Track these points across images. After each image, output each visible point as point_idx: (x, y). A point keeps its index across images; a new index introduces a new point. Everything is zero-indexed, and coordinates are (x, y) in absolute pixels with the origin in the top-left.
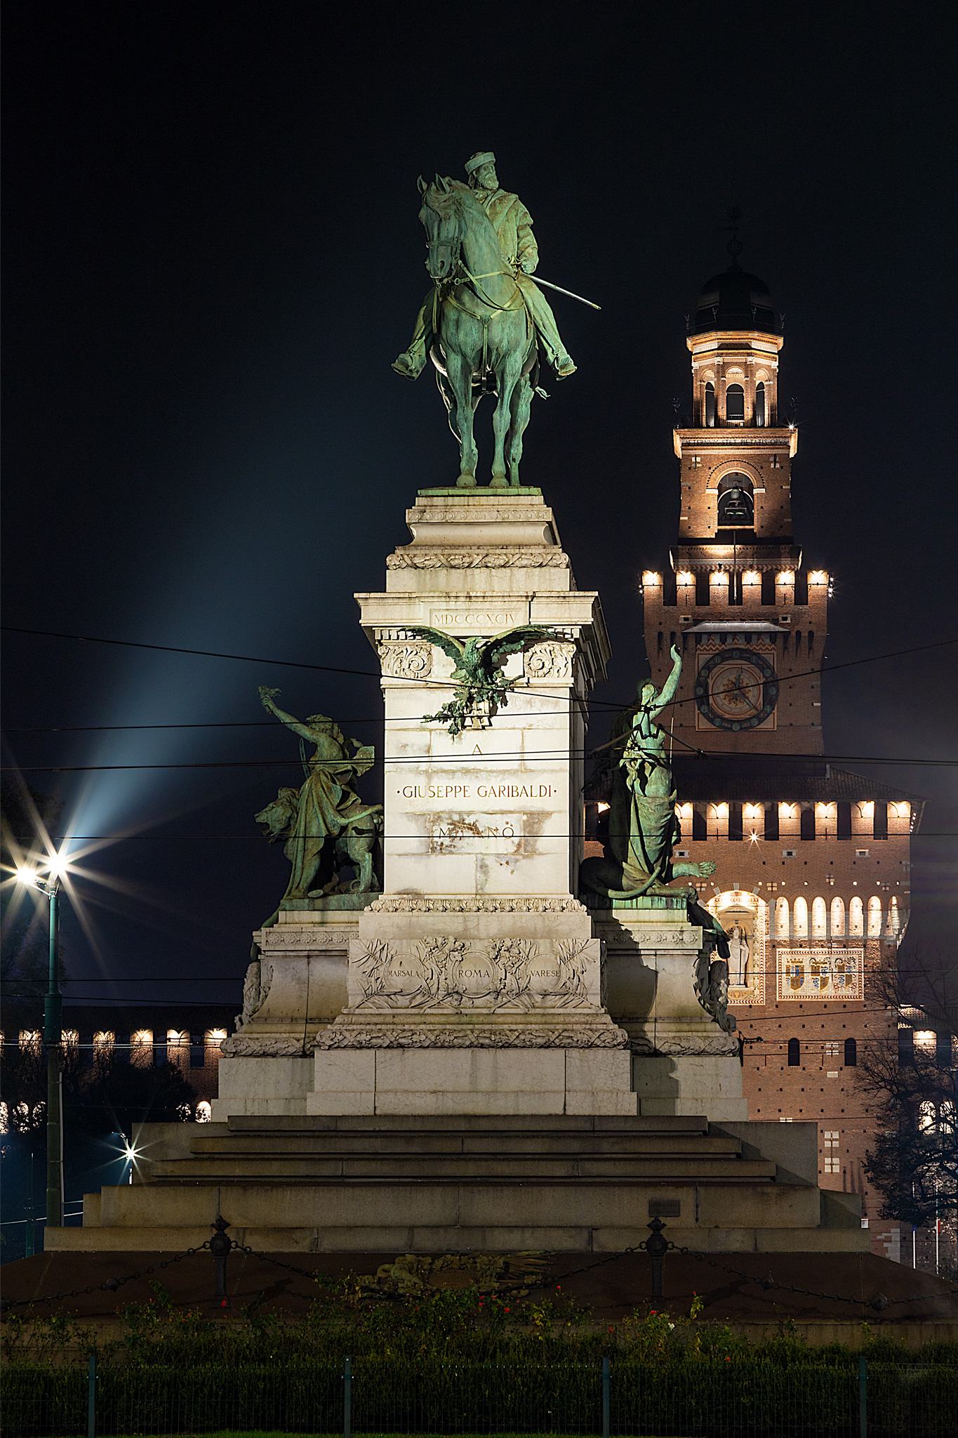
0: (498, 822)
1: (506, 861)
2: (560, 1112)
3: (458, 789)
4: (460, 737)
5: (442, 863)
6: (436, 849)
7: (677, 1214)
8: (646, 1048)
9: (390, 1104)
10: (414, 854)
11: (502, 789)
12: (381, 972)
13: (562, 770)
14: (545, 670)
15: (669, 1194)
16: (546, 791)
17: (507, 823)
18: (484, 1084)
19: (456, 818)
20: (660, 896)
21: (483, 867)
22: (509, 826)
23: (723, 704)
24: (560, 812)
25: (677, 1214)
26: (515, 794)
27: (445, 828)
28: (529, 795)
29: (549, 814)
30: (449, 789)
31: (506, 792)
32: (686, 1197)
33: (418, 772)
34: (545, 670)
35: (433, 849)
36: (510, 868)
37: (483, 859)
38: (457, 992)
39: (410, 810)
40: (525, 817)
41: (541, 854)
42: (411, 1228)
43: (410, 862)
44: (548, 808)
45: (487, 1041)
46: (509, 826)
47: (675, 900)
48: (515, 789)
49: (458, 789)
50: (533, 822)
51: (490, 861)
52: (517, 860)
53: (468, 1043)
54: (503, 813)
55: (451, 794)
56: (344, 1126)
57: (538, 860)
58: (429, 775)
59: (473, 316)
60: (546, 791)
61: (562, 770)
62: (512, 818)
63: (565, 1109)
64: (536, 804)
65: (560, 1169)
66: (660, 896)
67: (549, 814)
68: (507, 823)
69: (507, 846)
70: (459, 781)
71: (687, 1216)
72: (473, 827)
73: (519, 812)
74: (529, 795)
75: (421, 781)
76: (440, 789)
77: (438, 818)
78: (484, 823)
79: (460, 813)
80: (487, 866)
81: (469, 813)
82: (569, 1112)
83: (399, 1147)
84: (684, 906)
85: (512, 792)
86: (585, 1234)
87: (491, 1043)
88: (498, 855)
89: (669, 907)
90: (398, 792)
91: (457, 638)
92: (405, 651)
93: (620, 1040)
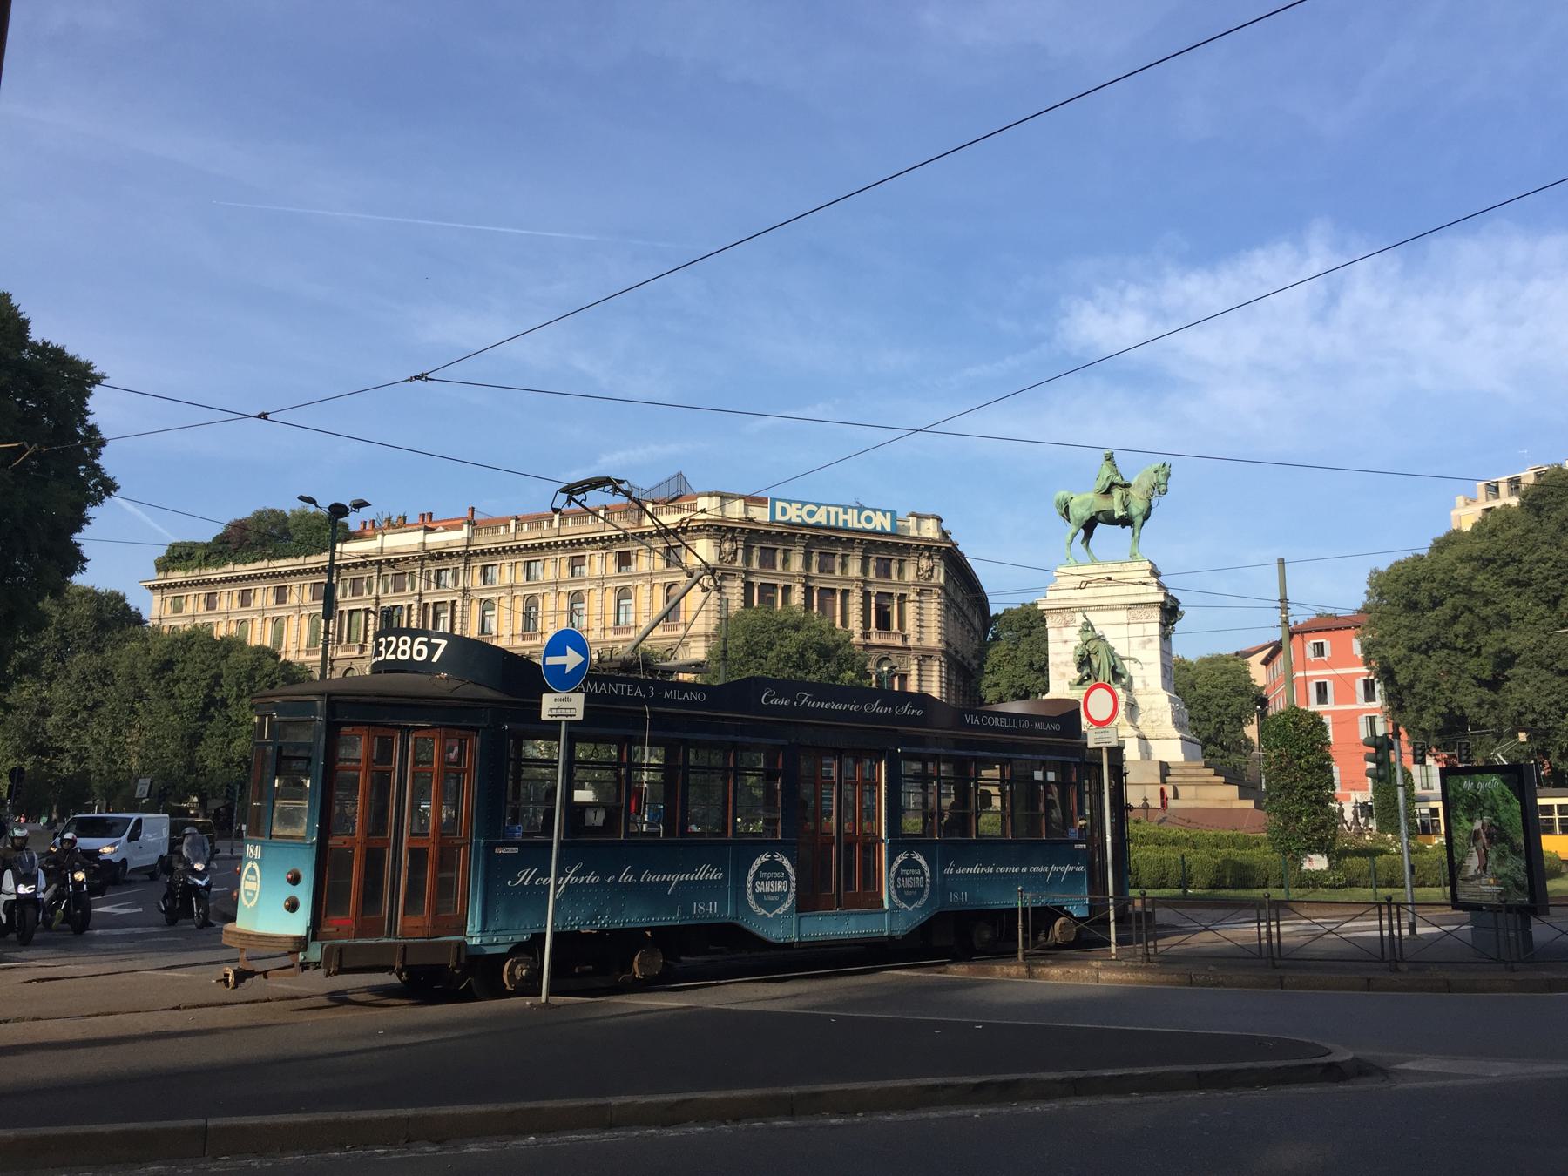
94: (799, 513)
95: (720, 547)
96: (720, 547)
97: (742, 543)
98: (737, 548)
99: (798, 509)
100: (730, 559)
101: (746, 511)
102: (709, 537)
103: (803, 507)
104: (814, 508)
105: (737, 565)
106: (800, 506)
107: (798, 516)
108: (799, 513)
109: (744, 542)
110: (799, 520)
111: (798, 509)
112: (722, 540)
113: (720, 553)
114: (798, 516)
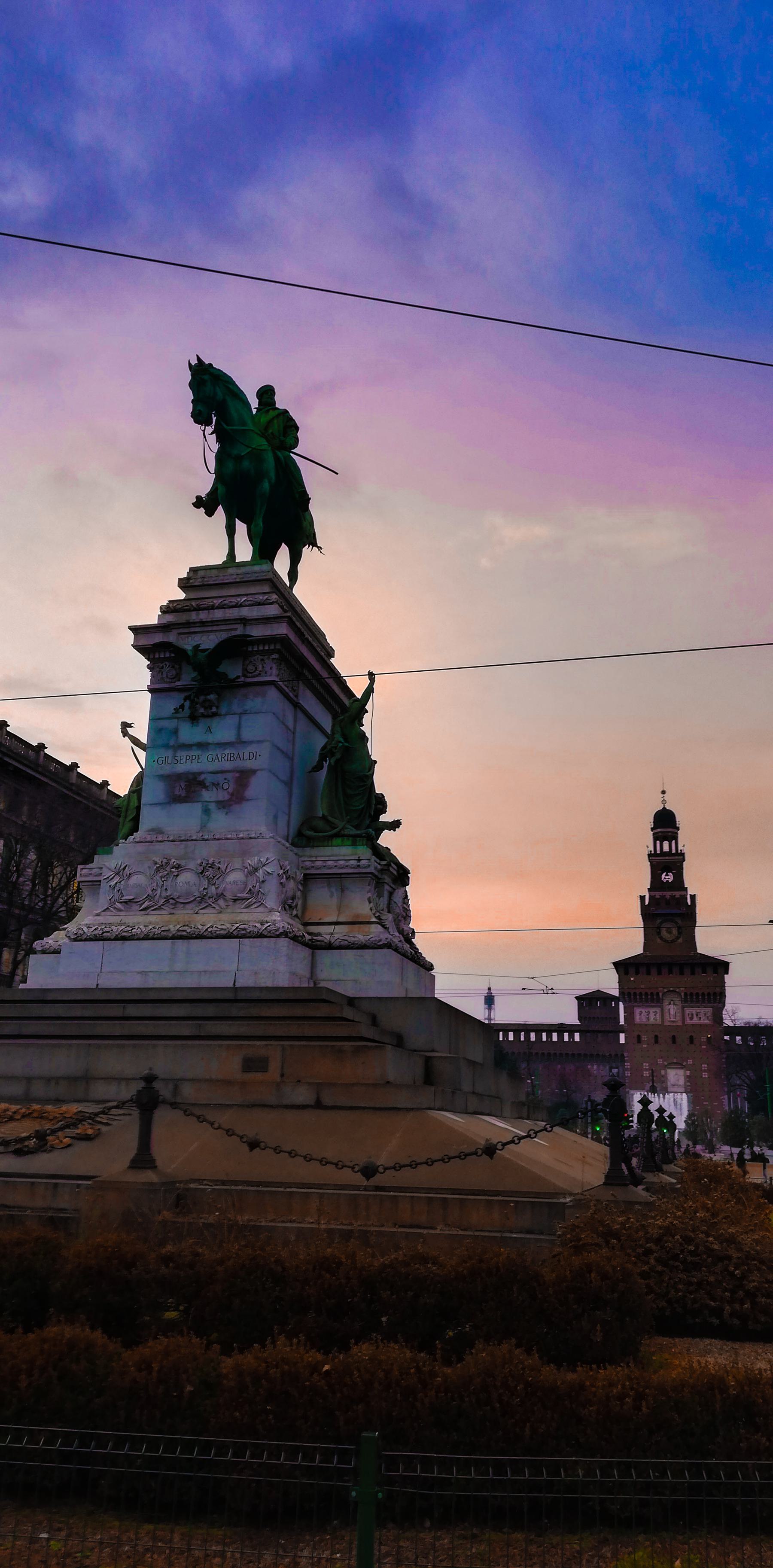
0: (220, 778)
1: (224, 805)
3: (194, 757)
4: (198, 722)
8: (323, 943)
9: (106, 982)
10: (160, 804)
11: (224, 756)
14: (257, 672)
15: (259, 1048)
17: (225, 779)
18: (179, 966)
19: (191, 777)
20: (348, 836)
21: (206, 811)
22: (226, 781)
23: (664, 933)
26: (232, 759)
28: (242, 759)
29: (253, 772)
30: (188, 758)
31: (226, 758)
34: (257, 672)
36: (226, 811)
37: (206, 806)
38: (172, 898)
39: (161, 772)
40: (237, 775)
41: (248, 800)
42: (29, 1080)
43: (158, 810)
46: (226, 781)
47: (358, 839)
48: (232, 755)
49: (194, 757)
50: (244, 777)
52: (231, 805)
53: (170, 935)
55: (189, 762)
56: (51, 997)
62: (229, 776)
63: (234, 984)
66: (348, 836)
67: (253, 772)
68: (225, 779)
69: (223, 796)
70: (195, 752)
72: (202, 785)
74: (242, 759)
75: (170, 753)
76: (182, 757)
78: (209, 779)
79: (194, 774)
80: (209, 810)
81: (201, 773)
82: (238, 985)
83: (78, 1011)
84: (365, 843)
86: (171, 1086)
87: (189, 935)
89: (354, 844)
90: (154, 761)
92: (165, 666)
93: (281, 930)
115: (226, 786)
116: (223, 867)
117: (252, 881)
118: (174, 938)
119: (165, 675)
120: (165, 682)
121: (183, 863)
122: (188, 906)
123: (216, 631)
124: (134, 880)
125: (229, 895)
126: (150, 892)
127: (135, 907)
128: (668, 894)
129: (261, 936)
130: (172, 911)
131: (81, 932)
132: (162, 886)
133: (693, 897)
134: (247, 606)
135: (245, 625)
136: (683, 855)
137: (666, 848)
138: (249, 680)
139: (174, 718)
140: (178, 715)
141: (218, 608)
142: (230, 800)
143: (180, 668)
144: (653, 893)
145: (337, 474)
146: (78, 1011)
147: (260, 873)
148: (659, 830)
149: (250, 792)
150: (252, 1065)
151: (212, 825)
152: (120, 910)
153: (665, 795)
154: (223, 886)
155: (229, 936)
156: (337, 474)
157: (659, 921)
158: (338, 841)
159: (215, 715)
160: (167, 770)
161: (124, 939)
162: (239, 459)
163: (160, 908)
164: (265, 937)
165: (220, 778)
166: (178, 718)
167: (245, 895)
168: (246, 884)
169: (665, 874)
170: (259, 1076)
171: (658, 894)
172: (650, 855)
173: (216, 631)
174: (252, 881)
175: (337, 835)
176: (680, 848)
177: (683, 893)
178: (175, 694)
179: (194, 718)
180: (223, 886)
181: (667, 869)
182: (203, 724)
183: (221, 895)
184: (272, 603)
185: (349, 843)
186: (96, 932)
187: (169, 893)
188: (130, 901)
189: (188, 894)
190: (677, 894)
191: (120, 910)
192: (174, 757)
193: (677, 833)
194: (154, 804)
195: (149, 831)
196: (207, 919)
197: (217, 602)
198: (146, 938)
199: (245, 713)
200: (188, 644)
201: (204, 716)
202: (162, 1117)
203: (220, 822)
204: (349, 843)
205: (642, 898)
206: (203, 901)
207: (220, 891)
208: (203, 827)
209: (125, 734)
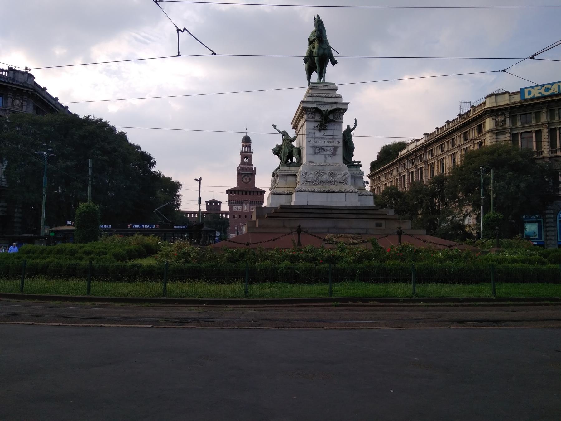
0: (328, 148)
1: (330, 156)
2: (345, 205)
5: (318, 156)
6: (316, 153)
7: (381, 226)
10: (311, 154)
12: (307, 177)
13: (341, 138)
15: (379, 221)
16: (338, 142)
19: (320, 147)
21: (325, 157)
23: (244, 180)
24: (341, 147)
25: (381, 226)
27: (318, 149)
29: (338, 147)
32: (383, 222)
33: (312, 138)
35: (316, 153)
36: (331, 157)
40: (334, 147)
42: (328, 228)
44: (339, 146)
45: (329, 191)
50: (335, 148)
51: (327, 156)
52: (332, 156)
54: (329, 146)
56: (304, 207)
57: (336, 156)
58: (315, 138)
59: (322, 48)
60: (338, 142)
61: (341, 138)
62: (331, 148)
64: (336, 145)
65: (353, 216)
67: (338, 147)
70: (321, 140)
71: (383, 227)
72: (324, 149)
73: (333, 146)
75: (313, 139)
77: (316, 147)
78: (326, 148)
79: (321, 146)
81: (323, 146)
83: (318, 211)
85: (332, 142)
88: (328, 155)
91: (323, 110)
94: (539, 91)
95: (496, 120)
96: (496, 120)
97: (508, 115)
98: (505, 118)
99: (538, 90)
100: (502, 124)
101: (510, 100)
102: (490, 116)
103: (541, 88)
104: (549, 86)
105: (507, 126)
106: (540, 87)
107: (539, 93)
108: (539, 91)
109: (509, 114)
110: (540, 95)
111: (538, 90)
112: (497, 116)
113: (496, 122)
114: (539, 93)
115: (330, 151)
116: (336, 174)
117: (344, 178)
118: (327, 192)
119: (310, 116)
120: (310, 118)
121: (324, 172)
122: (326, 184)
123: (328, 105)
124: (310, 176)
125: (338, 182)
126: (316, 179)
127: (311, 183)
128: (246, 166)
129: (351, 193)
130: (323, 185)
131: (300, 190)
132: (319, 178)
133: (255, 168)
134: (333, 98)
135: (336, 104)
136: (252, 152)
137: (246, 150)
138: (336, 120)
139: (313, 129)
140: (315, 128)
141: (324, 97)
142: (332, 155)
143: (315, 115)
144: (241, 166)
145: (339, 54)
146: (318, 211)
147: (346, 176)
148: (244, 143)
149: (337, 153)
150: (378, 225)
151: (327, 161)
152: (307, 184)
153: (247, 130)
154: (336, 179)
155: (342, 192)
156: (339, 54)
157: (243, 176)
158: (352, 167)
159: (326, 129)
160: (313, 144)
161: (312, 192)
162: (324, 49)
163: (318, 184)
164: (352, 193)
165: (328, 148)
166: (315, 130)
167: (342, 181)
168: (342, 178)
169: (245, 159)
170: (380, 228)
171: (243, 166)
172: (241, 152)
173: (328, 105)
174: (344, 178)
175: (352, 165)
176: (251, 150)
177: (251, 166)
178: (313, 123)
179: (320, 130)
180: (336, 179)
181: (247, 157)
182: (323, 132)
183: (336, 181)
184: (340, 98)
185: (355, 167)
186: (304, 190)
187: (321, 180)
188: (310, 181)
189: (327, 180)
190: (250, 166)
191: (307, 184)
192: (315, 141)
193: (250, 145)
194: (310, 154)
195: (309, 162)
196: (333, 188)
197: (324, 95)
198: (319, 192)
199: (335, 130)
200: (322, 108)
201: (323, 129)
202: (402, 236)
203: (330, 160)
204: (355, 167)
205: (238, 167)
206: (331, 182)
207: (335, 180)
208: (325, 162)
209: (275, 129)
